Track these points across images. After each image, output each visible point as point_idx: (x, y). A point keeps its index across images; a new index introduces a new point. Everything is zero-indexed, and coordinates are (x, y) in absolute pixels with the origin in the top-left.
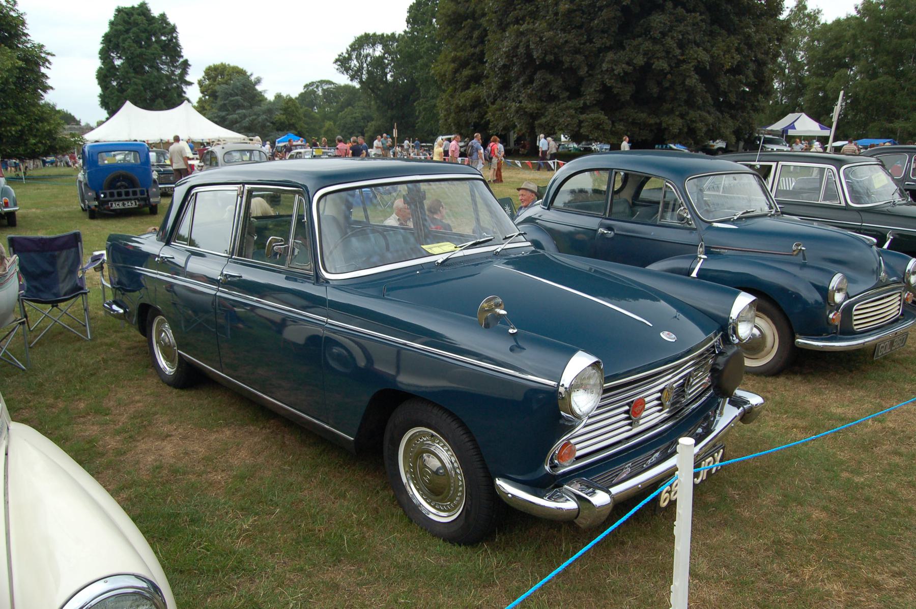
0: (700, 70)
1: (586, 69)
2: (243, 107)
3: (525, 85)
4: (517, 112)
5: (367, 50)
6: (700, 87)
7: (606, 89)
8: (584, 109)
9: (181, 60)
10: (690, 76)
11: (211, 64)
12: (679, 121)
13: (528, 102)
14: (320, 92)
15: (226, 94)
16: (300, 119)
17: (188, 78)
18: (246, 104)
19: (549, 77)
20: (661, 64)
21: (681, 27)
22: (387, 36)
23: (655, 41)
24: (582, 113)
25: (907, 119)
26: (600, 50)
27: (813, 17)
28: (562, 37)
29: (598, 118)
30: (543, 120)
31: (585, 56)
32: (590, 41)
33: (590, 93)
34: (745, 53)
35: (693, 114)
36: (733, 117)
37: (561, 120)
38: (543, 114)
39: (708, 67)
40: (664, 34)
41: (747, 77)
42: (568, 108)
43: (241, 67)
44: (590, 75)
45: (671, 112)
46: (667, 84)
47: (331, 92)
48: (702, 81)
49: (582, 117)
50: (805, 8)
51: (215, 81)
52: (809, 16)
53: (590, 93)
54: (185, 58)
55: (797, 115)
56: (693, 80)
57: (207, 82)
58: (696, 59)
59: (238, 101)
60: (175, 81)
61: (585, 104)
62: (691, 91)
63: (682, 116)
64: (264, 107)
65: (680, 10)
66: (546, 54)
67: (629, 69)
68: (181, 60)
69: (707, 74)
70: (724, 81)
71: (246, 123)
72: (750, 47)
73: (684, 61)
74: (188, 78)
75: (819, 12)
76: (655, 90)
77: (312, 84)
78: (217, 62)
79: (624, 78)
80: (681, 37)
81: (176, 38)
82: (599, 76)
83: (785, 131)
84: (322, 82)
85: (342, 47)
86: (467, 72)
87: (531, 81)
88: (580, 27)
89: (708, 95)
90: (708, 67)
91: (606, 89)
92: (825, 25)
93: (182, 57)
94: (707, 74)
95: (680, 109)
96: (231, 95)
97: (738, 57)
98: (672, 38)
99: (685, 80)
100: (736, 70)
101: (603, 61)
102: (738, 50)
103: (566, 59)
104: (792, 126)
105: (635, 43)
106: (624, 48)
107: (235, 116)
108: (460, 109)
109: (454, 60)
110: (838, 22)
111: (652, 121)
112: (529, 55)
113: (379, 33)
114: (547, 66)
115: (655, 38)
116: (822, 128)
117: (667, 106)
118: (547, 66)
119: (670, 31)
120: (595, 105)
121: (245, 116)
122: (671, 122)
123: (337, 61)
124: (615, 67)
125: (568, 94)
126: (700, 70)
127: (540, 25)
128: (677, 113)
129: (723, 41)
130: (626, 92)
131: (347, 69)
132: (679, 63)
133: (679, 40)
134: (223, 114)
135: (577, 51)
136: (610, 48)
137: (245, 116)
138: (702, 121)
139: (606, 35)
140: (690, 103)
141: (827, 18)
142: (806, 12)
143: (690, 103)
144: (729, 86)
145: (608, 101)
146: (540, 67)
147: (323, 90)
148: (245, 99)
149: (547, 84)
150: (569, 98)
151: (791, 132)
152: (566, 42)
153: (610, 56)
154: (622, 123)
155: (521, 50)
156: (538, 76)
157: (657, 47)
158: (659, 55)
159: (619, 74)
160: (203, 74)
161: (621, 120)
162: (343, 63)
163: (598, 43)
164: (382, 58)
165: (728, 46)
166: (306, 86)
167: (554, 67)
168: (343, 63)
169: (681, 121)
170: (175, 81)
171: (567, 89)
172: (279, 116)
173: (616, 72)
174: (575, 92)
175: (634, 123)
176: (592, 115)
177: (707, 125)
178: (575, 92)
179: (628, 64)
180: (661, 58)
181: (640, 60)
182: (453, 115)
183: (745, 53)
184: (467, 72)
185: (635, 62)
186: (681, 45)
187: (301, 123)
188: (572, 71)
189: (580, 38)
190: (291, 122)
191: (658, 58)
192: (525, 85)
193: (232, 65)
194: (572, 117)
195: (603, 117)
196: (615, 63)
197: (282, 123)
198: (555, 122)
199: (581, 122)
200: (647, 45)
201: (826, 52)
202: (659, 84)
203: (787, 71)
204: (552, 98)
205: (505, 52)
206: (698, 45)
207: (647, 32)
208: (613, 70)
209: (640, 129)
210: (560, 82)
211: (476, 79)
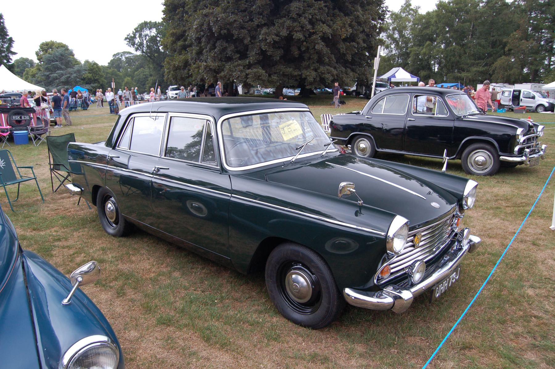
0: (324, 39)
1: (249, 39)
2: (61, 69)
3: (210, 50)
4: (205, 69)
5: (147, 32)
6: (326, 50)
7: (263, 53)
8: (249, 66)
9: (8, 37)
10: (318, 43)
11: (44, 41)
12: (314, 74)
13: (212, 62)
14: (123, 59)
15: (49, 60)
16: (102, 76)
17: (13, 50)
18: (63, 67)
19: (225, 44)
20: (298, 35)
21: (311, 11)
22: (159, 23)
23: (294, 20)
24: (248, 69)
25: (468, 71)
26: (258, 26)
27: (416, 11)
28: (232, 18)
29: (258, 72)
30: (222, 74)
31: (248, 30)
32: (251, 20)
34: (356, 28)
35: (322, 69)
36: (353, 70)
37: (234, 74)
38: (223, 70)
39: (330, 37)
40: (299, 15)
41: (358, 43)
42: (239, 65)
43: (64, 43)
44: (252, 43)
45: (307, 67)
46: (303, 49)
47: (131, 59)
48: (327, 46)
49: (248, 71)
50: (410, 5)
51: (46, 52)
52: (412, 10)
54: (10, 36)
55: (397, 68)
56: (320, 46)
57: (42, 53)
58: (322, 31)
59: (56, 64)
60: (4, 52)
61: (249, 62)
62: (319, 53)
63: (316, 70)
64: (76, 68)
66: (221, 30)
67: (277, 39)
68: (8, 37)
69: (328, 41)
70: (342, 47)
71: (63, 79)
72: (359, 24)
73: (314, 33)
74: (13, 50)
75: (419, 7)
76: (296, 53)
77: (118, 54)
78: (48, 40)
79: (275, 45)
80: (311, 17)
81: (3, 23)
82: (258, 44)
83: (389, 79)
84: (124, 53)
85: (130, 31)
86: (180, 43)
87: (214, 47)
88: (245, 11)
89: (333, 56)
90: (330, 37)
91: (263, 53)
92: (421, 15)
93: (8, 35)
94: (328, 41)
95: (314, 65)
96: (53, 61)
97: (350, 30)
98: (305, 18)
99: (315, 46)
100: (352, 38)
101: (260, 34)
102: (350, 26)
103: (235, 32)
104: (394, 76)
105: (281, 21)
106: (274, 25)
107: (55, 75)
108: (177, 69)
109: (173, 35)
110: (428, 13)
111: (296, 73)
112: (210, 29)
113: (153, 21)
114: (220, 37)
115: (293, 18)
116: (412, 77)
117: (305, 64)
119: (304, 13)
120: (255, 64)
121: (62, 75)
122: (308, 73)
123: (126, 39)
124: (267, 38)
125: (238, 55)
126: (324, 39)
127: (217, 10)
128: (312, 68)
129: (341, 20)
130: (277, 54)
131: (133, 44)
132: (311, 34)
133: (310, 19)
134: (48, 73)
135: (242, 28)
136: (265, 25)
137: (62, 75)
138: (329, 73)
139: (261, 17)
140: (320, 61)
141: (423, 12)
142: (411, 7)
143: (320, 61)
144: (346, 49)
145: (265, 61)
146: (218, 39)
147: (126, 58)
148: (62, 64)
149: (224, 50)
150: (240, 59)
151: (393, 80)
152: (235, 21)
153: (264, 30)
154: (276, 75)
155: (205, 26)
156: (218, 44)
157: (295, 24)
158: (296, 29)
159: (270, 42)
160: (39, 48)
161: (275, 73)
162: (131, 40)
163: (256, 22)
164: (156, 37)
165: (344, 24)
166: (114, 55)
167: (228, 37)
168: (131, 40)
169: (315, 73)
170: (4, 52)
171: (238, 52)
172: (88, 75)
173: (268, 41)
174: (243, 55)
175: (284, 75)
176: (255, 70)
177: (333, 75)
178: (243, 55)
179: (277, 35)
180: (298, 31)
181: (284, 33)
182: (172, 72)
183: (356, 28)
184: (180, 43)
185: (281, 34)
186: (311, 22)
187: (103, 79)
188: (241, 41)
189: (245, 18)
190: (96, 78)
191: (296, 31)
192: (210, 50)
193: (58, 42)
194: (241, 71)
195: (261, 71)
196: (268, 36)
197: (89, 79)
198: (230, 75)
199: (247, 75)
200: (288, 23)
201: (421, 31)
202: (299, 49)
203: (400, 43)
204: (229, 59)
205: (196, 29)
206: (324, 23)
207: (287, 14)
208: (266, 40)
209: (289, 79)
210: (233, 47)
211: (185, 47)
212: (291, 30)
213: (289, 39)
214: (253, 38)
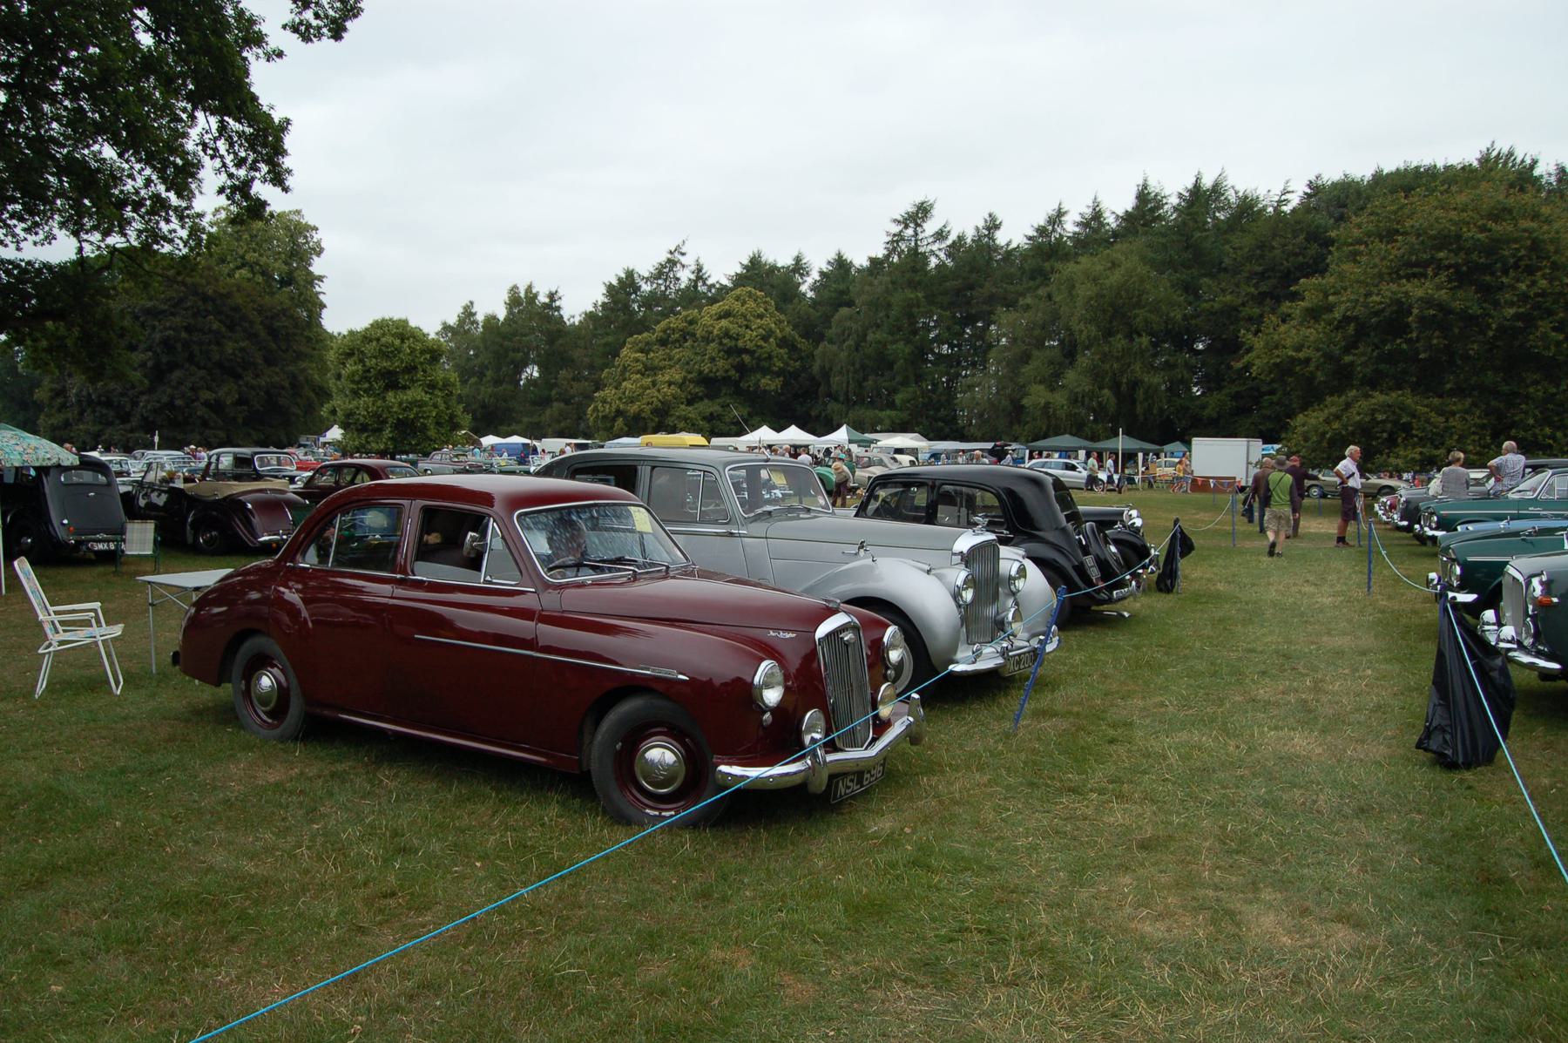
0: (206, 404)
7: (144, 419)
8: (132, 431)
33: (134, 422)
53: (134, 422)
62: (201, 417)
65: (193, 368)
91: (144, 419)
118: (99, 403)
153: (144, 398)
167: (108, 404)
174: (125, 418)
178: (125, 418)
181: (165, 399)
184: (60, 400)
186: (193, 389)
200: (169, 391)
204: (111, 424)
211: (63, 407)
212: (172, 398)
213: (171, 405)
214: (135, 404)
